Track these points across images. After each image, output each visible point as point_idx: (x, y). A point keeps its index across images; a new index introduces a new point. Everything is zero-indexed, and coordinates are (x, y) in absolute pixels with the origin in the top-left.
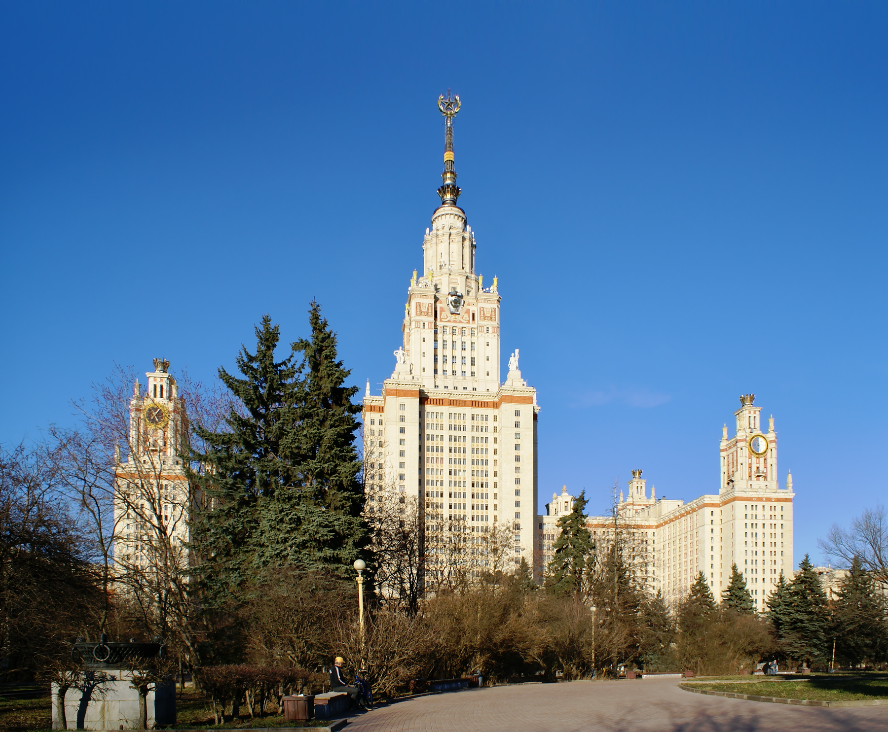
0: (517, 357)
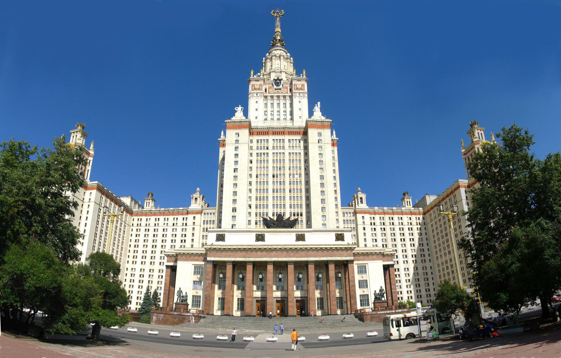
0: (319, 106)
